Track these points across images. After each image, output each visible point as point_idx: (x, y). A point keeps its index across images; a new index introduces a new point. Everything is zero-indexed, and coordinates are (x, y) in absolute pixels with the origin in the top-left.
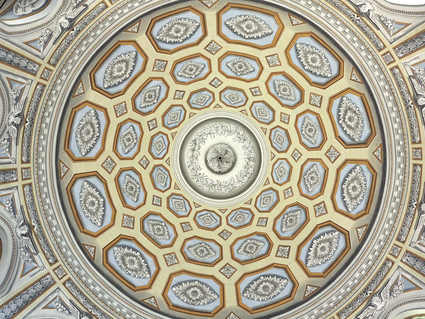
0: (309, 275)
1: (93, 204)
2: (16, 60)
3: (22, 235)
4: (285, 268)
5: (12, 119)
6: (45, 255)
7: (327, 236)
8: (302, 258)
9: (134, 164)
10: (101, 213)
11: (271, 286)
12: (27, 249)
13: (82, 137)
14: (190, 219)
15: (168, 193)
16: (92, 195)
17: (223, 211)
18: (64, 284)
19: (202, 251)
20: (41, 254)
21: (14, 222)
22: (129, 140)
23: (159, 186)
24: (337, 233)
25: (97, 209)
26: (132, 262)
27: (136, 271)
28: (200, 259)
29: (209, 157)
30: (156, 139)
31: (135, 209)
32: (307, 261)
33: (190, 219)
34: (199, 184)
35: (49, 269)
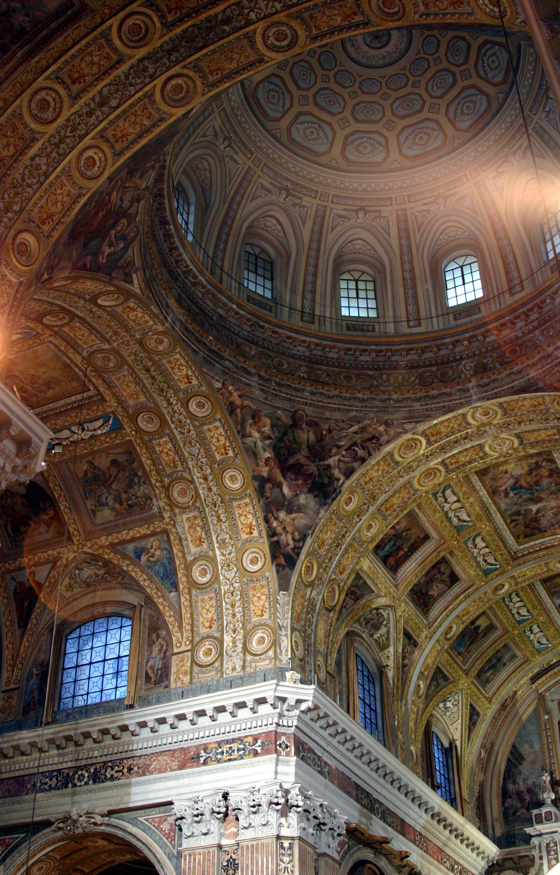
0: (494, 85)
1: (312, 133)
2: (196, 124)
3: (285, 199)
4: (474, 86)
5: (222, 147)
6: (307, 195)
7: (491, 52)
8: (482, 73)
9: (320, 85)
10: (322, 135)
11: (471, 105)
12: (295, 204)
13: (272, 103)
14: (384, 89)
15: (357, 85)
16: (307, 128)
17: (404, 69)
18: (332, 202)
19: (408, 105)
20: (305, 198)
21: (274, 198)
22: (304, 75)
23: (347, 85)
24: (497, 47)
25: (318, 134)
26: (366, 147)
27: (372, 151)
28: (410, 112)
29: (368, 41)
30: (322, 59)
31: (342, 112)
32: (487, 75)
33: (384, 89)
34: (374, 62)
35: (315, 202)
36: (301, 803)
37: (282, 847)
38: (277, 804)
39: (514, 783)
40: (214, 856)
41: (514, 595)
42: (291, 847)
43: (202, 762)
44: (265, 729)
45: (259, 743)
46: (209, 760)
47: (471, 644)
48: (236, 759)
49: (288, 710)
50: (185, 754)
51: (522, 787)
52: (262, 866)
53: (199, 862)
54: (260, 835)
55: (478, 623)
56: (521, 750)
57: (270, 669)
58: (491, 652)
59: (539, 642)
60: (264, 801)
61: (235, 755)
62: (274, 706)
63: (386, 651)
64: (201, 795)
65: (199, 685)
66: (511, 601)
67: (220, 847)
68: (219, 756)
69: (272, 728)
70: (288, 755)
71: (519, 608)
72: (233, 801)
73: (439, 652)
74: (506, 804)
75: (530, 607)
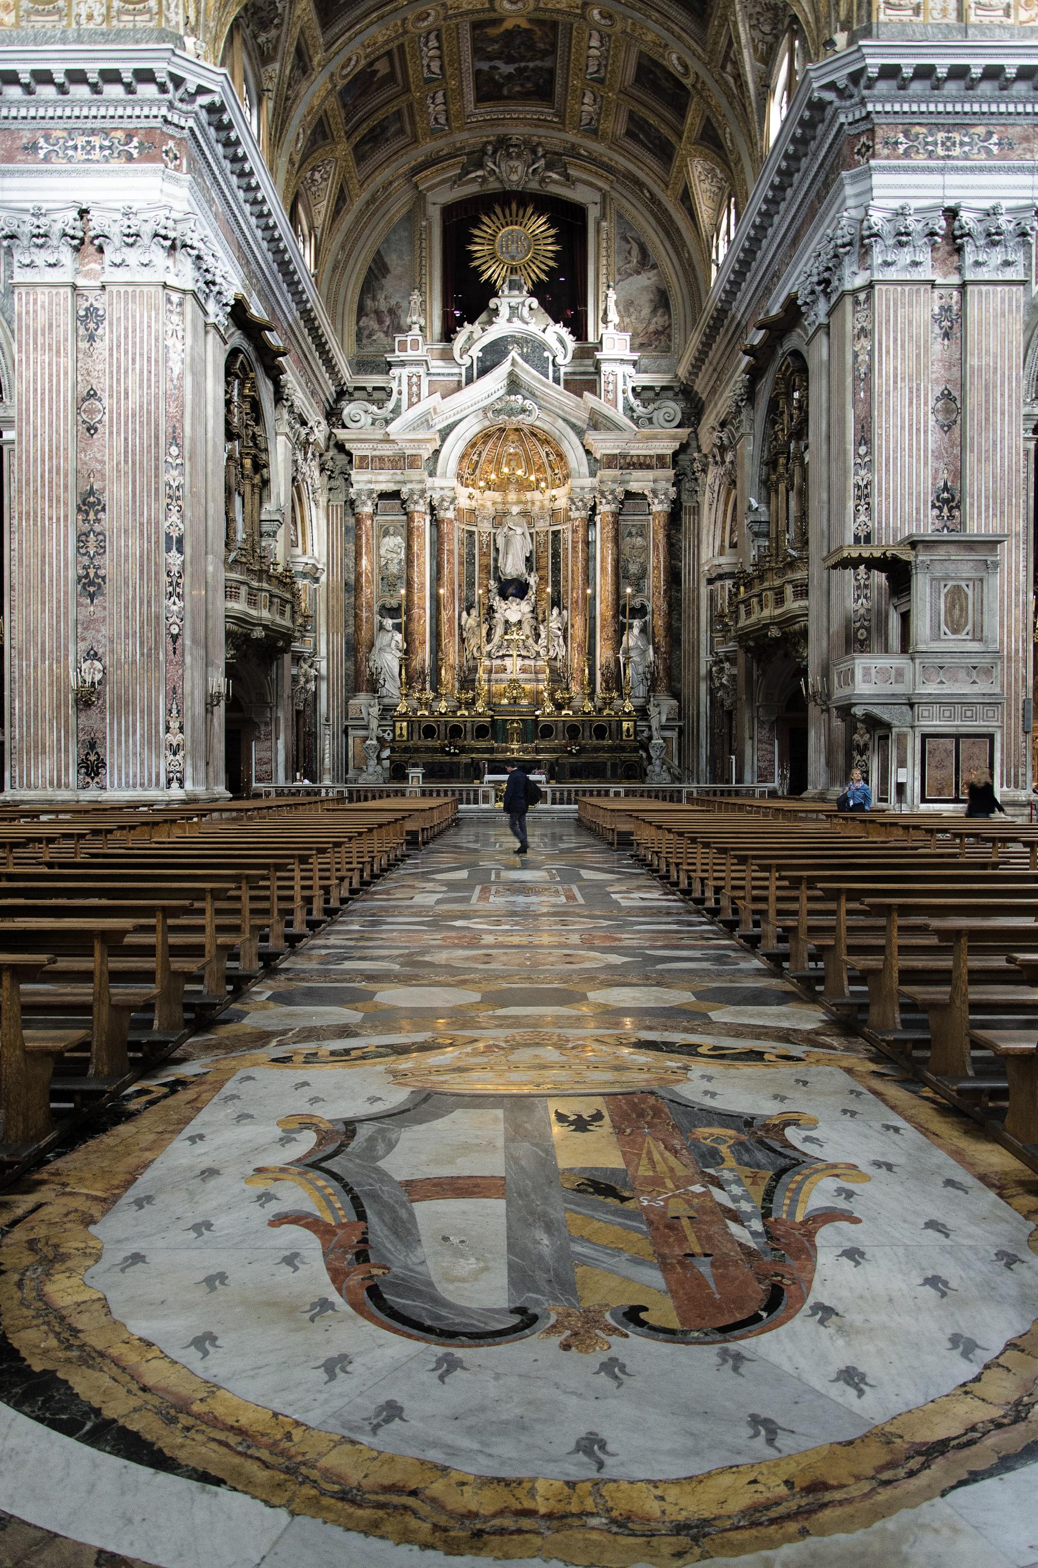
36: (196, 244)
37: (169, 301)
38: (165, 238)
39: (374, 299)
40: (66, 298)
41: (432, 36)
42: (181, 304)
43: (41, 156)
44: (144, 123)
45: (135, 142)
46: (54, 155)
47: (360, 96)
48: (98, 161)
49: (182, 100)
50: (13, 140)
51: (383, 306)
52: (141, 322)
53: (43, 307)
54: (137, 278)
55: (378, 66)
56: (386, 259)
57: (152, 30)
58: (380, 115)
59: (436, 119)
60: (147, 230)
61: (97, 154)
62: (163, 88)
63: (270, 68)
64: (45, 206)
65: (31, 32)
66: (426, 44)
67: (74, 287)
68: (70, 153)
69: (158, 123)
70: (177, 168)
71: (432, 58)
72: (97, 222)
73: (329, 93)
74: (361, 324)
75: (446, 59)
